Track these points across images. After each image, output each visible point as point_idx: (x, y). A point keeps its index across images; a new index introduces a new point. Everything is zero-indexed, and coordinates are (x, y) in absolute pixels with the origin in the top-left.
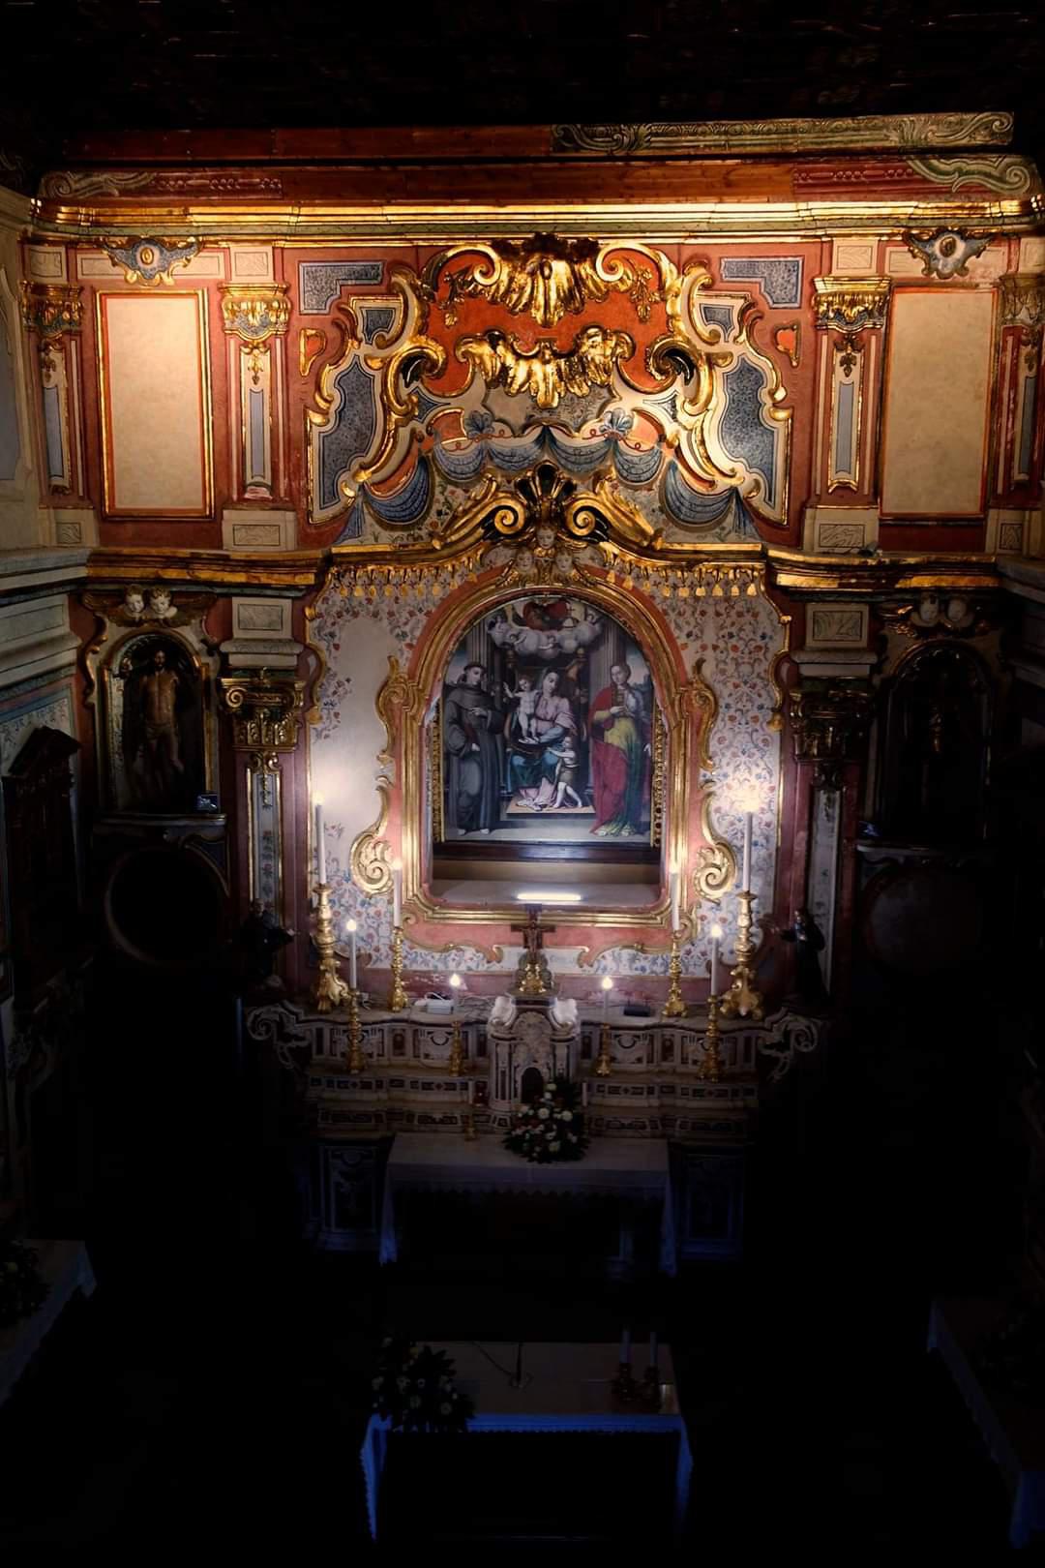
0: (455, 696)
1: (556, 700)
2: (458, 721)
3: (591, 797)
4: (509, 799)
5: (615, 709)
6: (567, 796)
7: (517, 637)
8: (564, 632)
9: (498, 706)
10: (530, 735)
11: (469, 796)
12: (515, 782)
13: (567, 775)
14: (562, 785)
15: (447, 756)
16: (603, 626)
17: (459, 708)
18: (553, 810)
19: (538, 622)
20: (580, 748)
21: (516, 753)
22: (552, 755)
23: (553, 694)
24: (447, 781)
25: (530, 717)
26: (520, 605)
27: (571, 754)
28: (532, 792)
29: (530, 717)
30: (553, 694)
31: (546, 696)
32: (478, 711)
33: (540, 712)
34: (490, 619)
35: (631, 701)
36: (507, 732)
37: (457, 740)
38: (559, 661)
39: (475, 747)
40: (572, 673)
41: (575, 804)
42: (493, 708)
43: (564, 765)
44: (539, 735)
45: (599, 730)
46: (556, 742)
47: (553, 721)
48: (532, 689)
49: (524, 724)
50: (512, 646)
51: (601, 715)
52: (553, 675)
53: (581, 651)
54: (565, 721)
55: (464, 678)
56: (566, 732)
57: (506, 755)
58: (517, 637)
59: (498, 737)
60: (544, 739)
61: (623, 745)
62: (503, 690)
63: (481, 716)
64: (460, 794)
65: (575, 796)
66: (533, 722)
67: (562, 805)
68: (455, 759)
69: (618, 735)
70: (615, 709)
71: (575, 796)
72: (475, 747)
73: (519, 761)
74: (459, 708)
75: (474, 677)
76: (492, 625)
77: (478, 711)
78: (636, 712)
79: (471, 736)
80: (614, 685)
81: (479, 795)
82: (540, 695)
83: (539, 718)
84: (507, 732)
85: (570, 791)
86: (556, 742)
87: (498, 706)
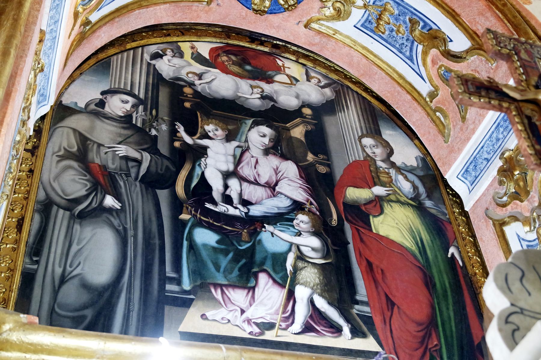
0: (79, 122)
1: (274, 161)
2: (81, 153)
3: (368, 321)
4: (186, 304)
5: (379, 190)
6: (316, 315)
7: (200, 76)
8: (275, 87)
9: (163, 148)
10: (228, 200)
11: (85, 286)
12: (198, 273)
13: (310, 275)
14: (302, 293)
15: (46, 208)
16: (337, 93)
17: (84, 141)
18: (288, 336)
19: (235, 69)
20: (331, 236)
21: (200, 224)
22: (274, 239)
23: (267, 152)
24: (36, 249)
25: (226, 175)
26: (204, 48)
27: (316, 242)
28: (238, 296)
29: (226, 175)
30: (267, 152)
31: (256, 151)
32: (123, 150)
33: (246, 170)
34: (153, 49)
35: (406, 186)
36: (180, 189)
37: (73, 183)
38: (274, 116)
39: (110, 201)
40: (298, 132)
41: (337, 330)
42: (153, 150)
43: (301, 257)
44: (246, 203)
45: (360, 214)
46: (281, 218)
47: (272, 187)
48: (229, 138)
49: (216, 183)
50: (191, 85)
51: (355, 194)
52: (265, 129)
53: (307, 111)
54: (293, 188)
55: (101, 104)
56: (297, 207)
57: (179, 227)
58: (200, 76)
59: (163, 195)
60: (256, 211)
61: (409, 243)
62: (173, 132)
63: (126, 158)
64: (63, 280)
65: (333, 314)
66: (234, 183)
67: (307, 329)
68: (61, 217)
69: (396, 225)
70: (379, 190)
71: (333, 314)
72: (110, 201)
73: (206, 237)
74: (84, 141)
75: (118, 105)
76: (157, 56)
77: (123, 150)
78: (416, 198)
79: (103, 180)
80: (369, 160)
81: (113, 287)
82: (245, 150)
83: (242, 179)
84: (180, 189)
85: (321, 304)
86: (281, 218)
87: (163, 148)
